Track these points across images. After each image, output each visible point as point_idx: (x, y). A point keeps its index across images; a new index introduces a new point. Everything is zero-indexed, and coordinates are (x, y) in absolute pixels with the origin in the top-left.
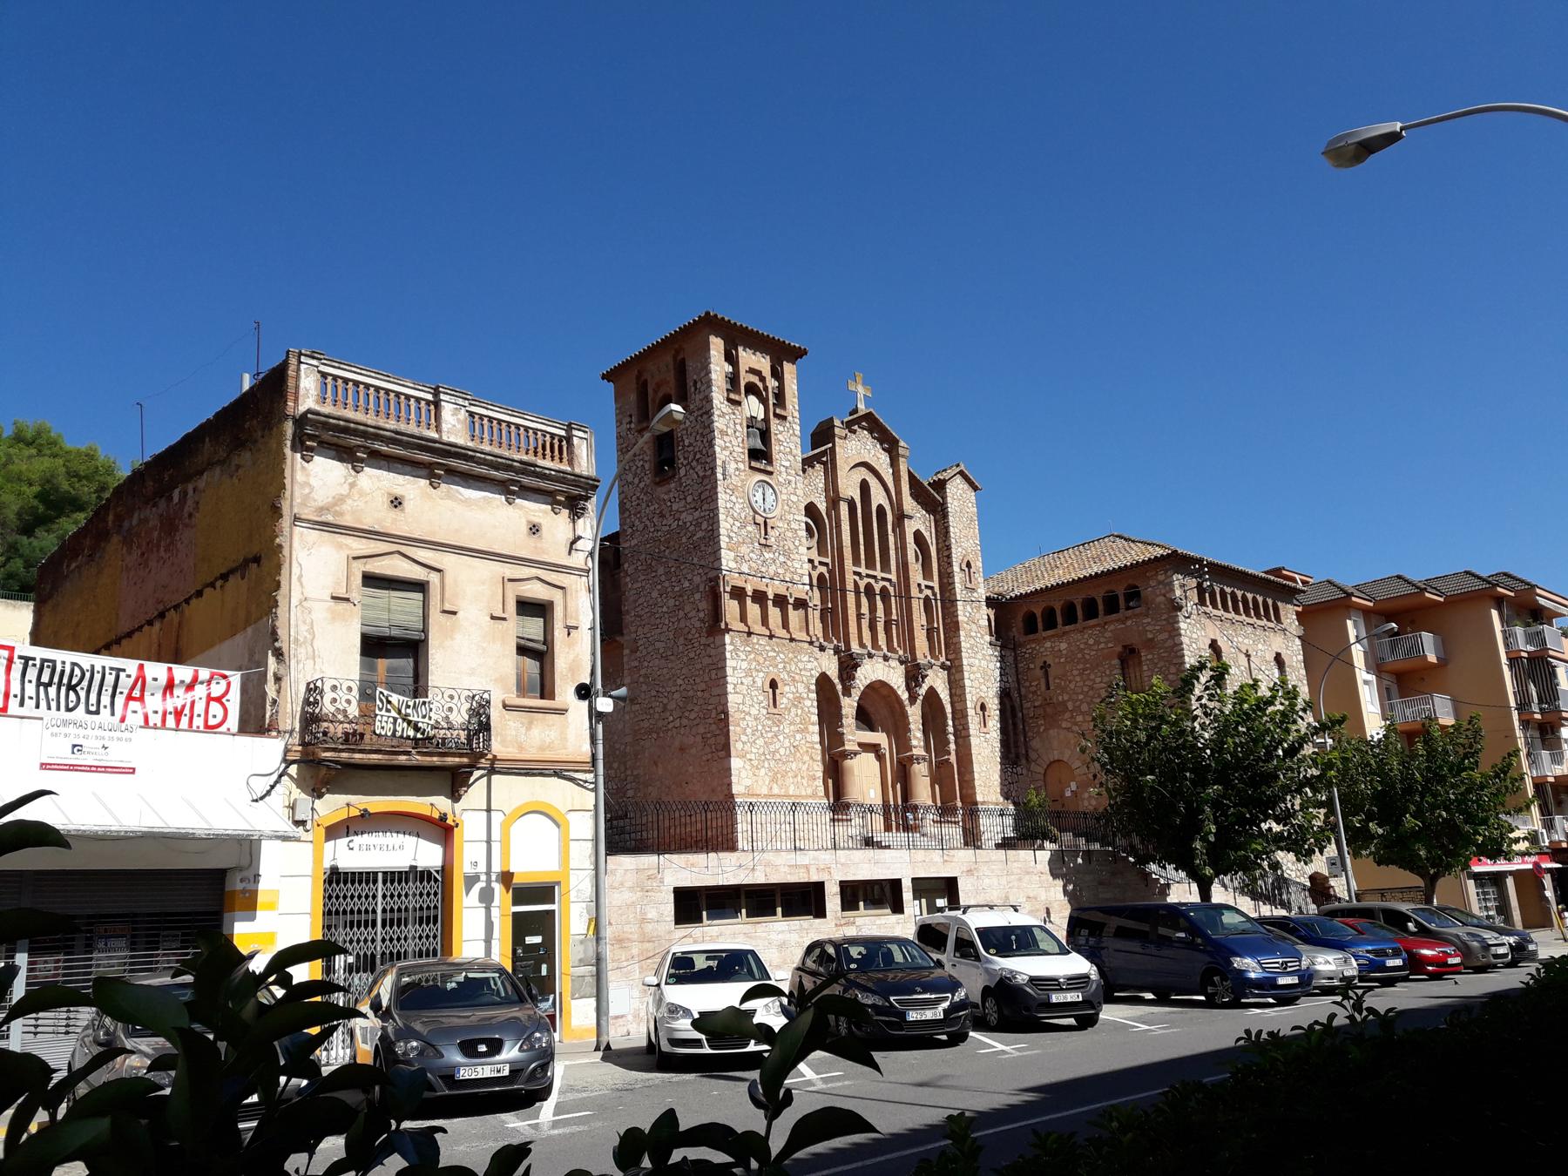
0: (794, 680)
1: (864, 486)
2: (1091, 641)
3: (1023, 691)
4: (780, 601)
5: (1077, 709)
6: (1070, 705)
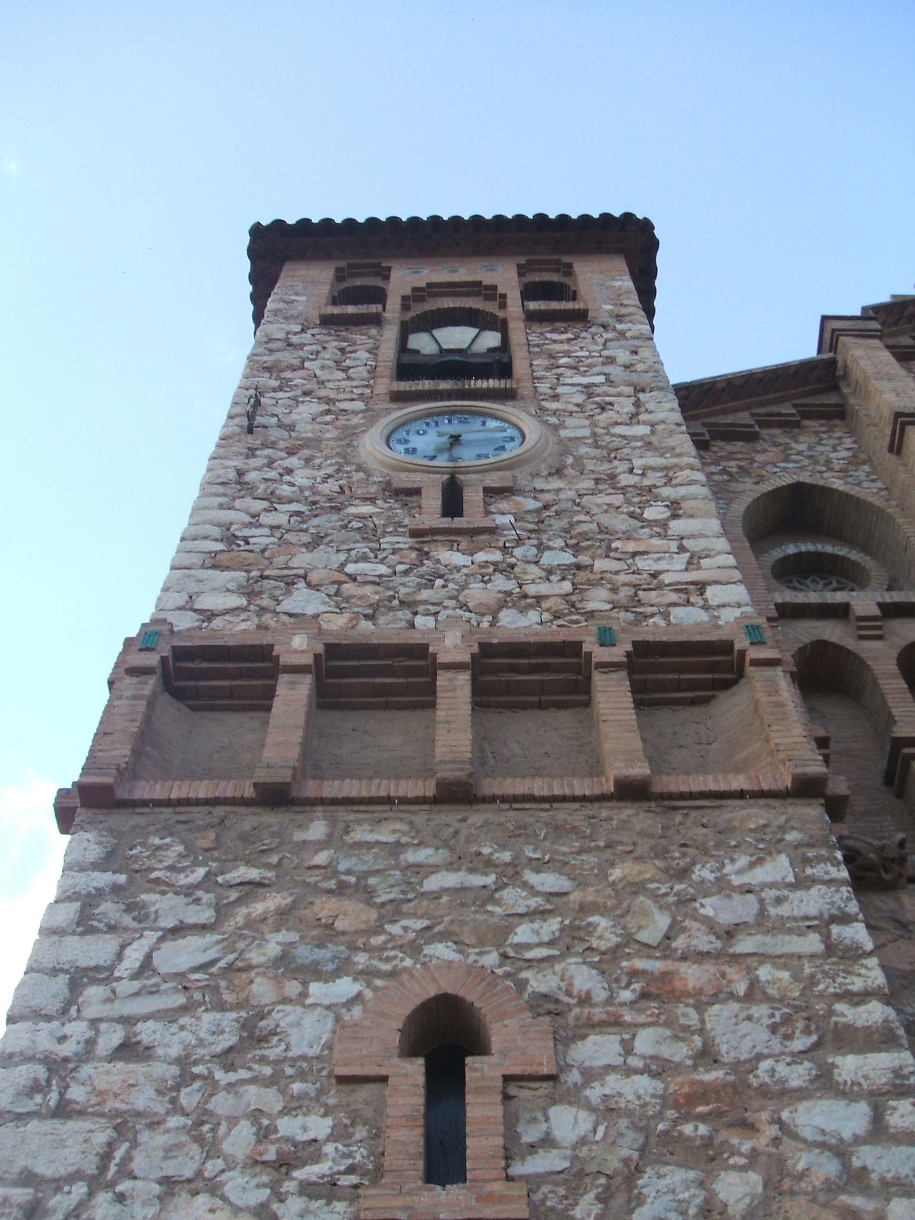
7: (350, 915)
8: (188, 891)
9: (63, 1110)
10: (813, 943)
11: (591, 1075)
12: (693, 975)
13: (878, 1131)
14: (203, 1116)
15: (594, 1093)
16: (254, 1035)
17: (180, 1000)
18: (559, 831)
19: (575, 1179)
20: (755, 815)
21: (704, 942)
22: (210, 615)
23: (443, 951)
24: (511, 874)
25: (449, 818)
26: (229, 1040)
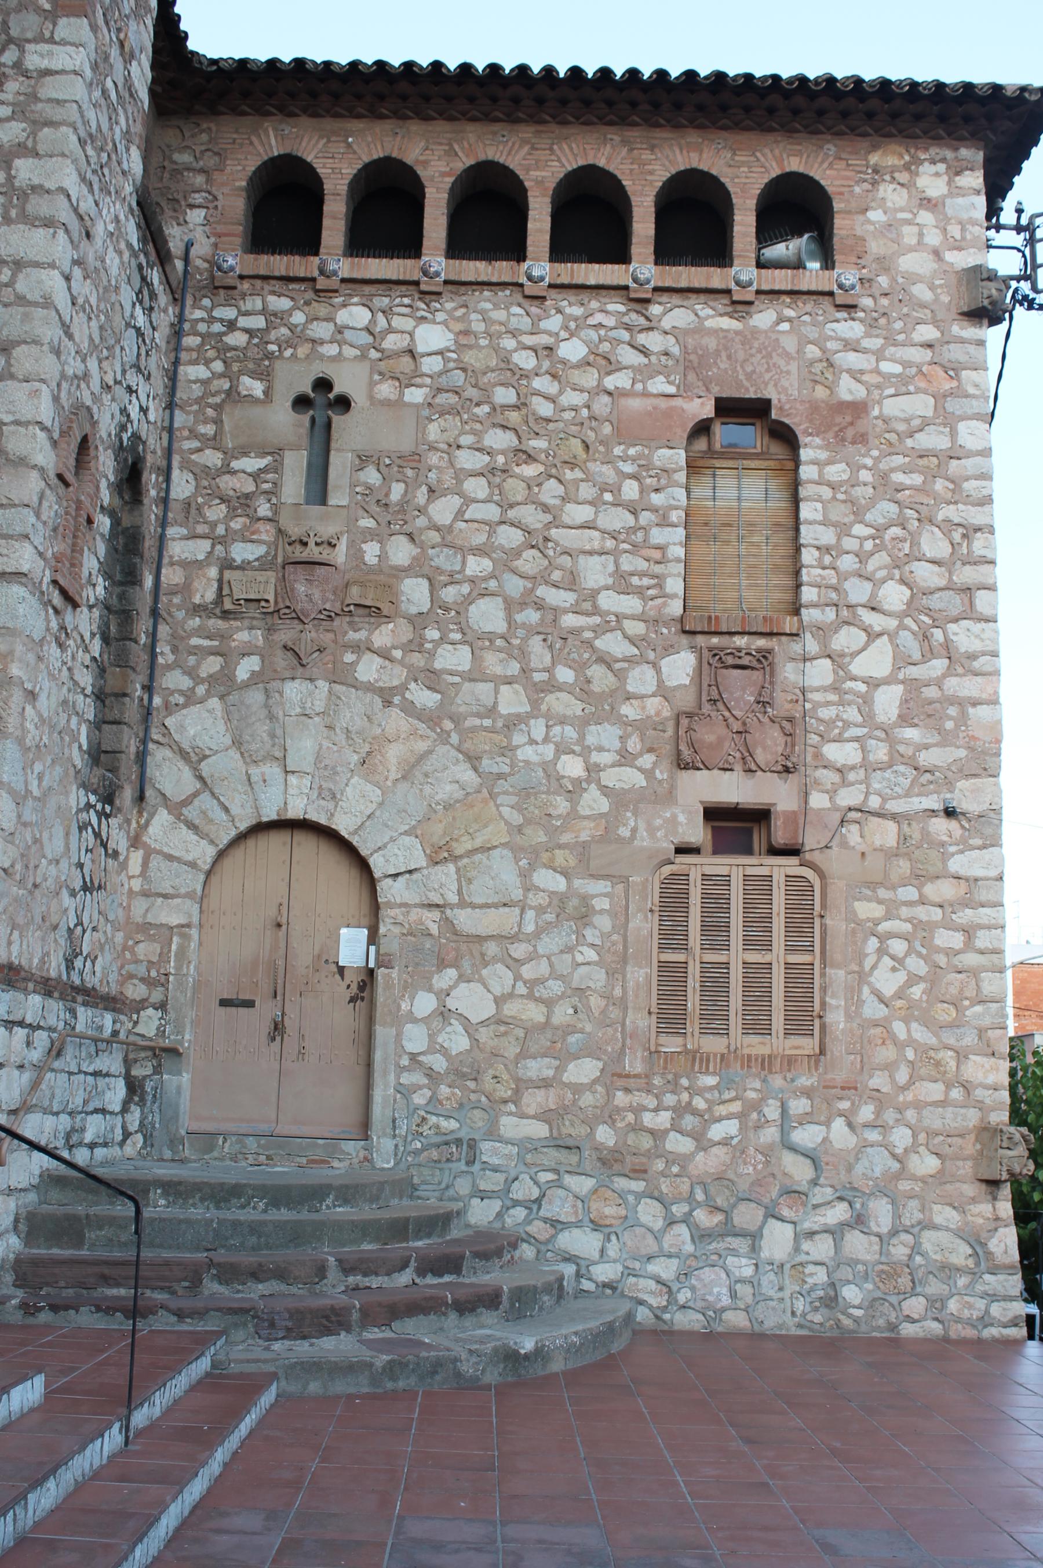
2: (573, 350)
3: (182, 486)
5: (447, 616)
6: (415, 593)
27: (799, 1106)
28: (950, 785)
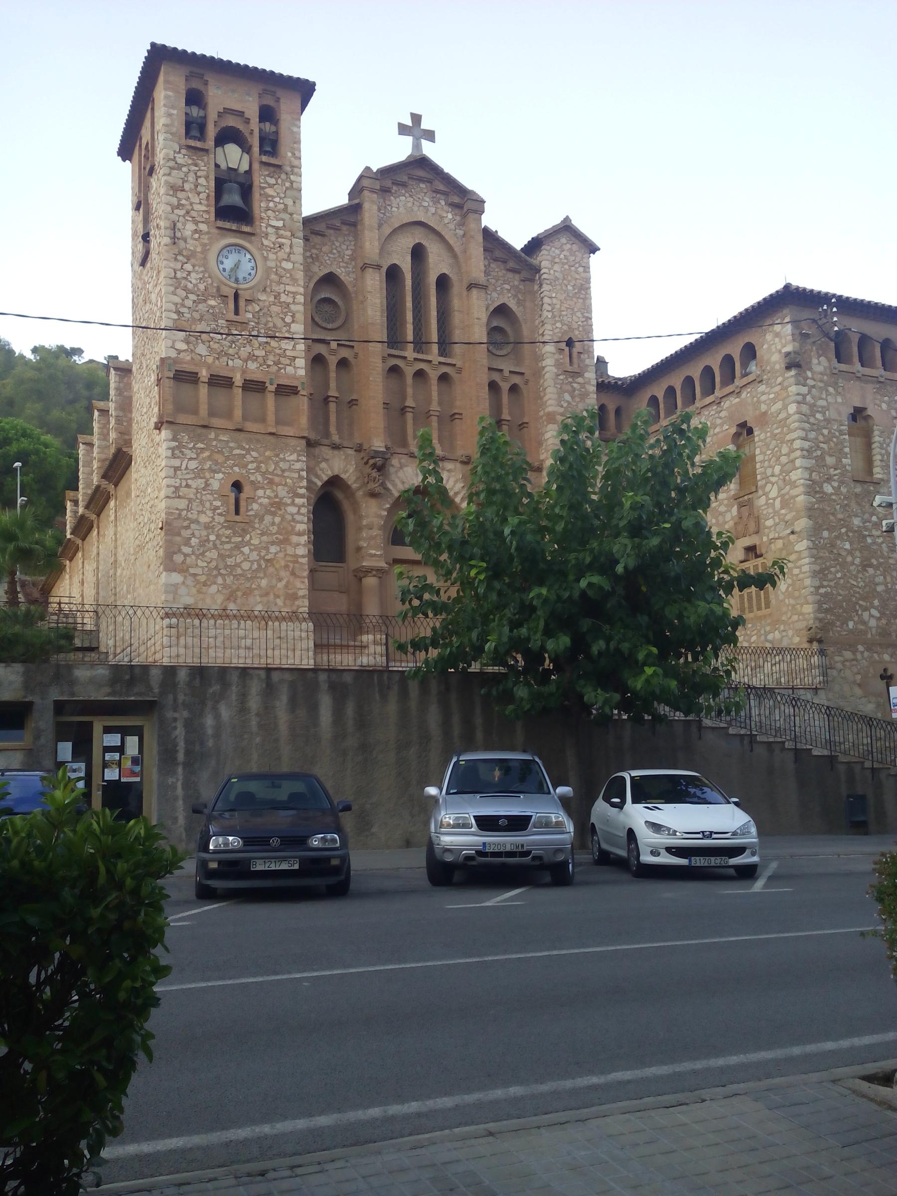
0: (271, 482)
1: (418, 253)
4: (253, 387)
7: (220, 459)
8: (190, 449)
9: (179, 497)
10: (296, 475)
11: (260, 497)
12: (277, 479)
13: (298, 513)
14: (201, 501)
15: (259, 501)
16: (207, 485)
17: (193, 476)
18: (258, 441)
19: (255, 516)
20: (293, 442)
21: (280, 473)
22: (179, 352)
23: (236, 469)
24: (248, 451)
25: (237, 434)
26: (203, 486)
27: (768, 628)
28: (793, 524)
